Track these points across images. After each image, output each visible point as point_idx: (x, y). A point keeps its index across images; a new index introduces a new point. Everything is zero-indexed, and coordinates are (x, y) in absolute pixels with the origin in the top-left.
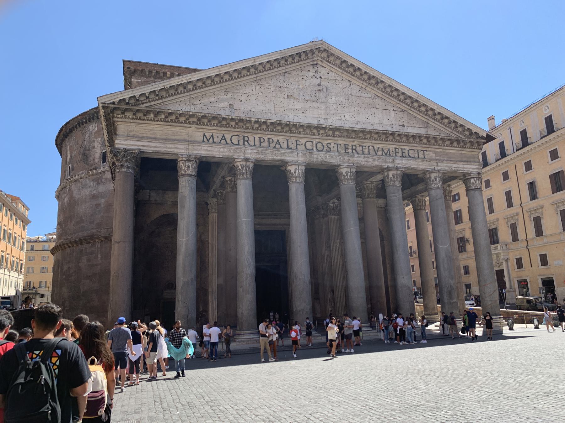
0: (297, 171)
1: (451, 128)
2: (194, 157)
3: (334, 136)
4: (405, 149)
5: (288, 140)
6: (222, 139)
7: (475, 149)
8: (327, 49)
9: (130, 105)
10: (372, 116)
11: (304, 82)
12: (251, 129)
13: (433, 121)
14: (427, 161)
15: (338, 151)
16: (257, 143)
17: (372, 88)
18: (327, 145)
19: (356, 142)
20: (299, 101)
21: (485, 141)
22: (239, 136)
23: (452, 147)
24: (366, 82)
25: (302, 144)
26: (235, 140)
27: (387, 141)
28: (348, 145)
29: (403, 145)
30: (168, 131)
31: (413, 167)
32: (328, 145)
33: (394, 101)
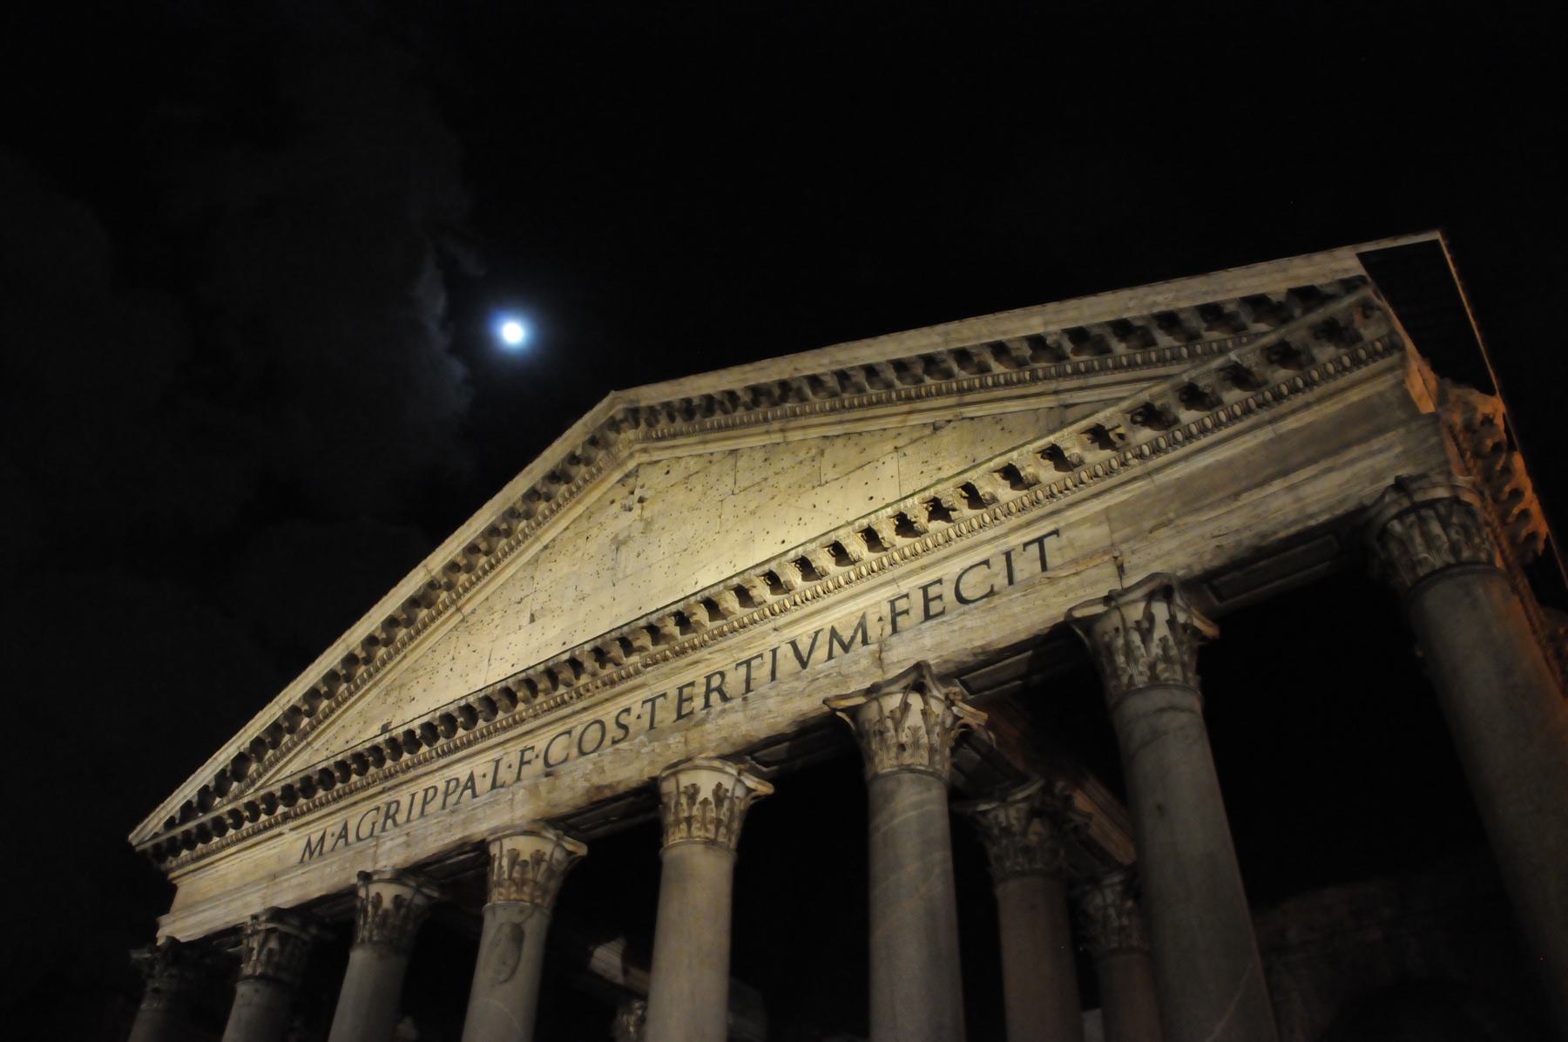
2: (263, 918)
3: (629, 676)
4: (939, 581)
6: (340, 837)
7: (1345, 369)
10: (802, 522)
12: (400, 774)
15: (652, 726)
16: (416, 811)
17: (803, 421)
19: (718, 657)
22: (378, 809)
23: (1189, 437)
25: (537, 756)
28: (692, 684)
29: (924, 568)
31: (977, 643)
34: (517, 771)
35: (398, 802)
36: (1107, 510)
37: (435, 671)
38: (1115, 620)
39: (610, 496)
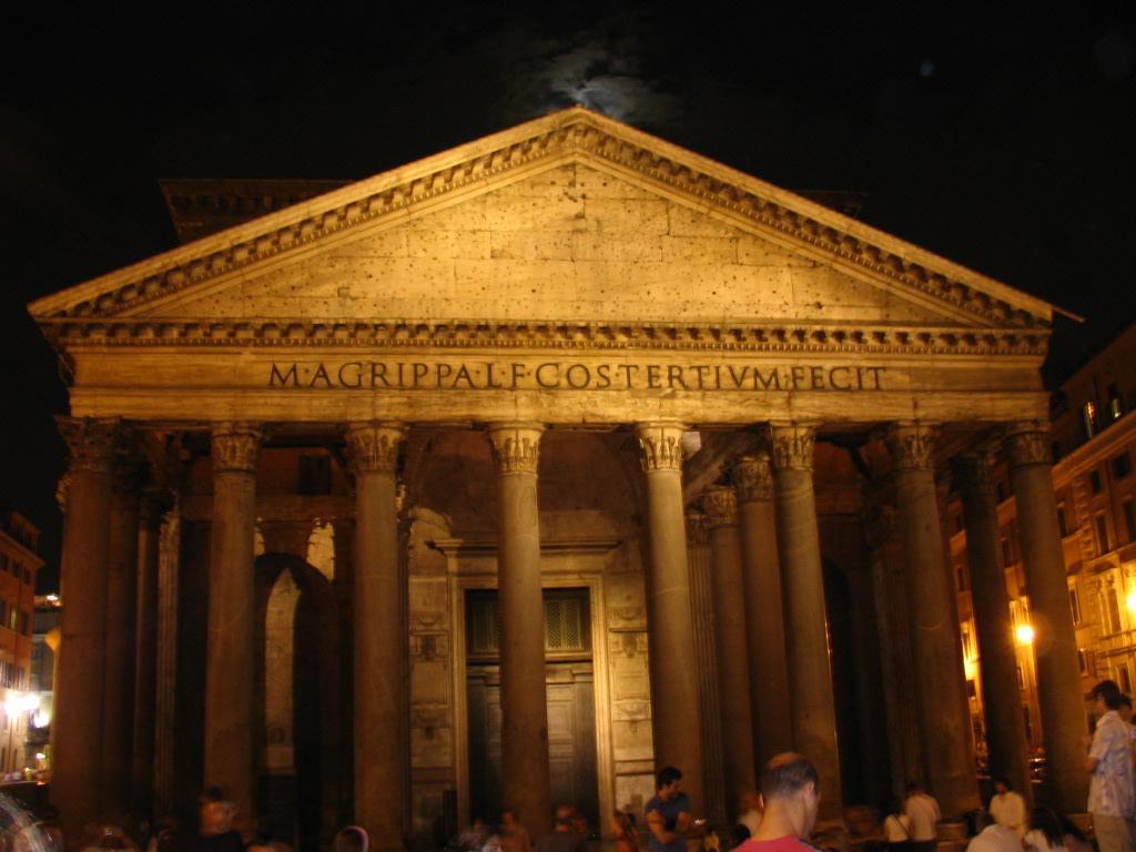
0: (513, 445)
1: (954, 302)
2: (244, 425)
3: (616, 347)
4: (820, 368)
5: (490, 366)
6: (317, 376)
7: (1024, 354)
8: (595, 126)
9: (102, 313)
11: (538, 212)
13: (904, 287)
14: (884, 398)
16: (408, 380)
17: (727, 211)
18: (599, 372)
19: (680, 358)
20: (522, 261)
21: (1049, 332)
22: (360, 364)
23: (956, 353)
24: (708, 198)
25: (529, 374)
26: (350, 378)
27: (767, 349)
28: (658, 367)
29: (816, 359)
30: (190, 366)
31: (844, 414)
32: (603, 371)
33: (788, 244)
34: (511, 378)
35: (384, 367)
36: (909, 368)
37: (388, 258)
38: (914, 431)
39: (550, 176)
